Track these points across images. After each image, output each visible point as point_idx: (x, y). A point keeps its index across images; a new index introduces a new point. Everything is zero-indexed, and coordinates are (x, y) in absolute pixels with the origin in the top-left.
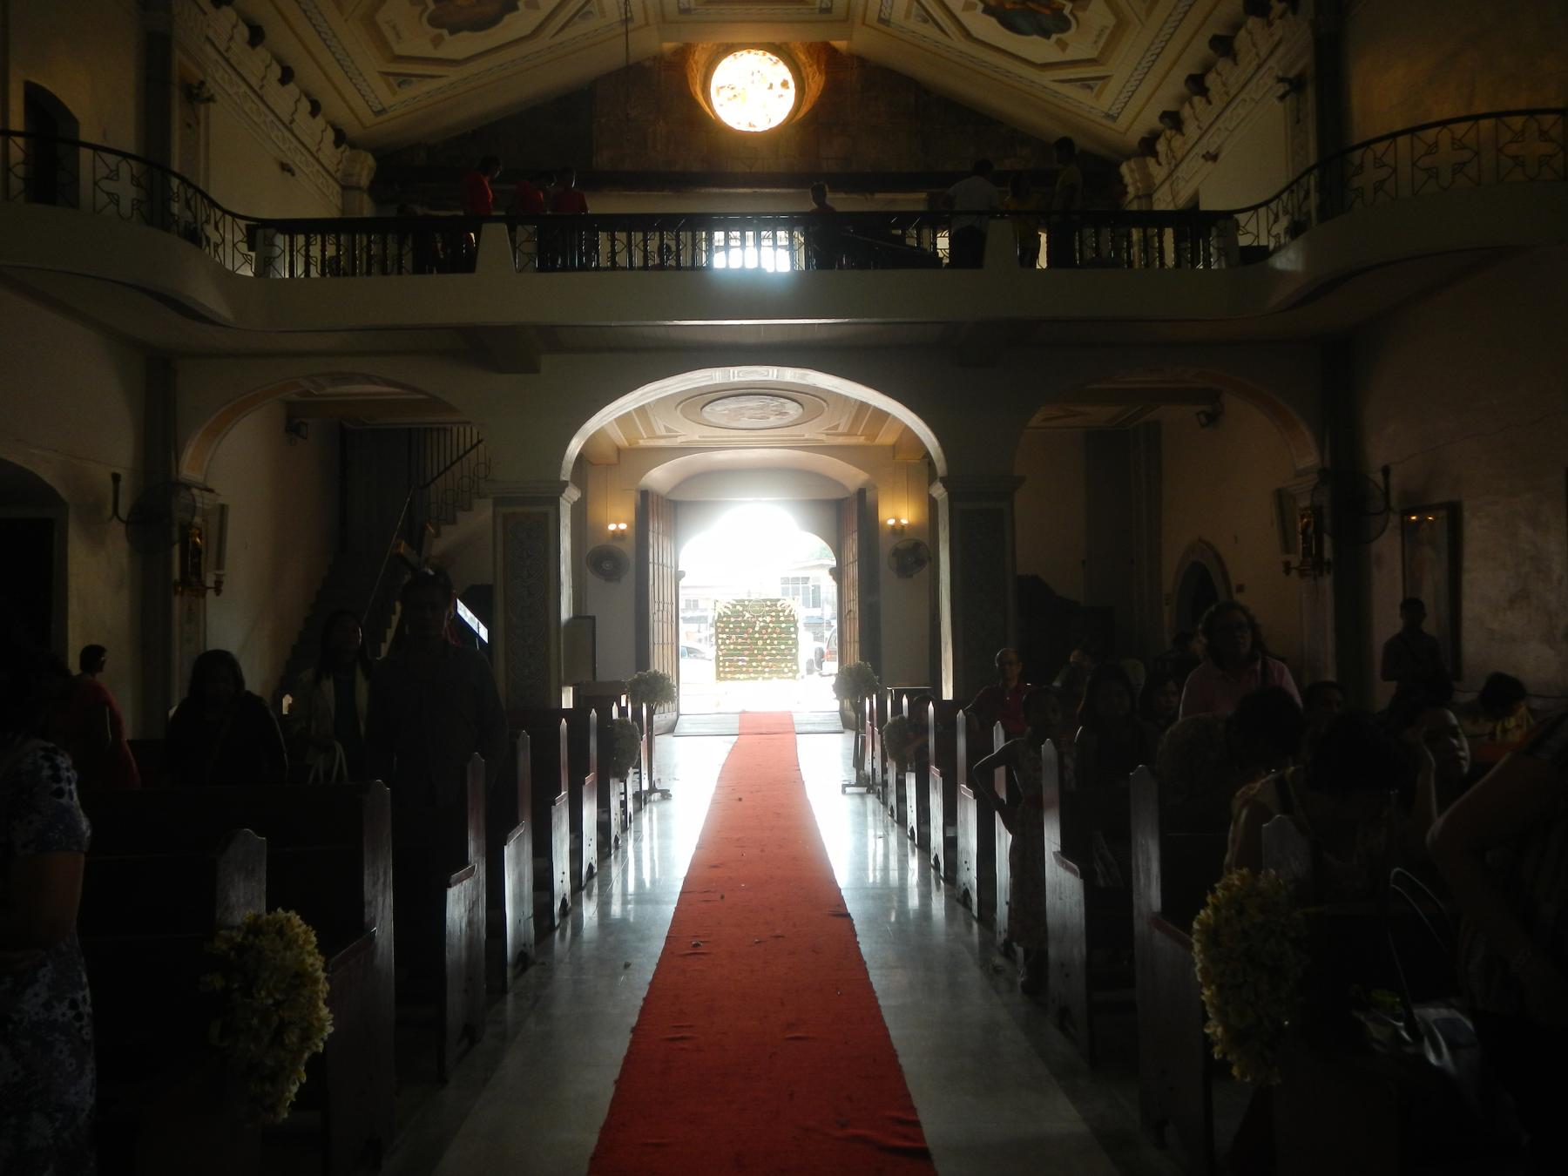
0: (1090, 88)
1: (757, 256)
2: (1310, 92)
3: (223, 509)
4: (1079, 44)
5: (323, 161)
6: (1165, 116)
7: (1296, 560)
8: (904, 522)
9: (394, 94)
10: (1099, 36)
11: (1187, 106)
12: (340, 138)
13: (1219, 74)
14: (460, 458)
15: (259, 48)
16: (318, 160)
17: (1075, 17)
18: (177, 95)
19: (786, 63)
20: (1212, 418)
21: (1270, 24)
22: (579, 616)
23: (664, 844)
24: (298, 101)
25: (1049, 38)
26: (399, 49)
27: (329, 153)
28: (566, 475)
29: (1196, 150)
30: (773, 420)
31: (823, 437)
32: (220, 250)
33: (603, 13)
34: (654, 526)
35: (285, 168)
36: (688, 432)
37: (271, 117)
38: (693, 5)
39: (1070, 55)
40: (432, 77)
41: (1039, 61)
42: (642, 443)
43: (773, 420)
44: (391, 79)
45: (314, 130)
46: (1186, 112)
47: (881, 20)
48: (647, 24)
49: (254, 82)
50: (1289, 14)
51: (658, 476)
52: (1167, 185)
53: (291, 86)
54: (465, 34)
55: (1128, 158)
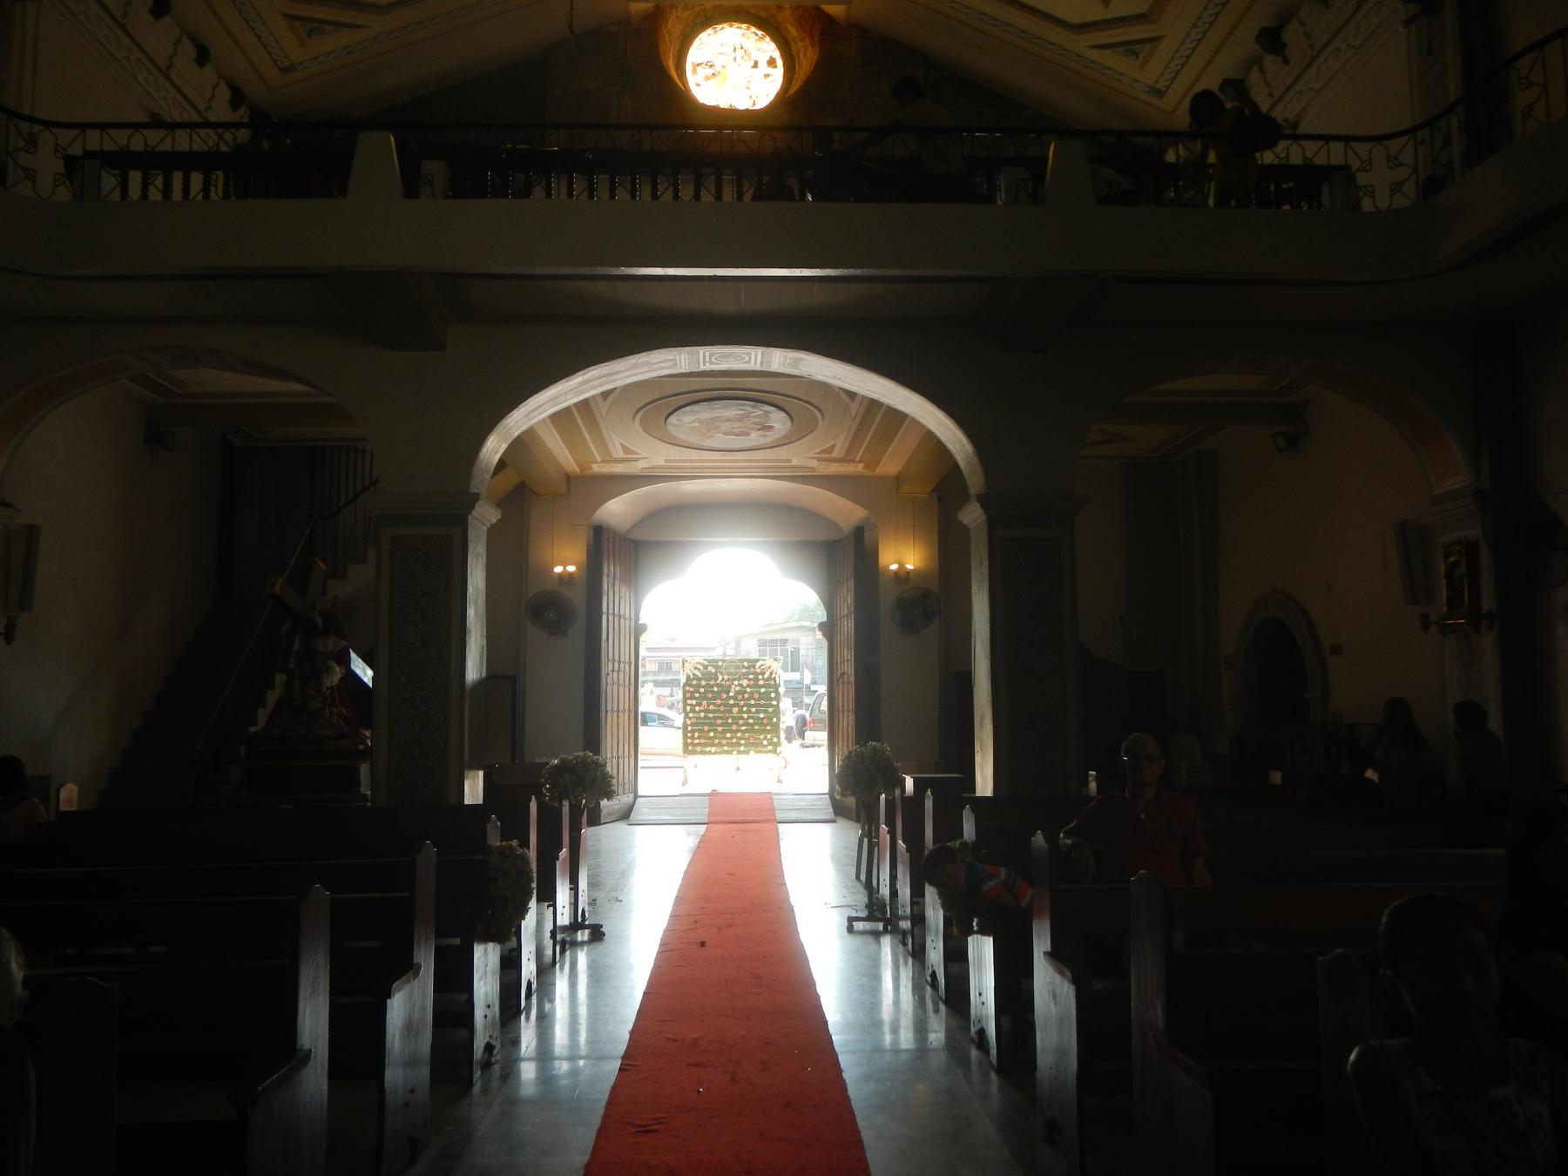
0: (1136, 54)
3: (32, 532)
8: (910, 567)
11: (1256, 69)
13: (1301, 23)
19: (773, 39)
22: (492, 678)
30: (755, 438)
31: (814, 463)
34: (609, 570)
36: (652, 454)
40: (352, 26)
42: (597, 468)
43: (755, 438)
44: (297, 23)
51: (617, 510)
53: (167, 20)
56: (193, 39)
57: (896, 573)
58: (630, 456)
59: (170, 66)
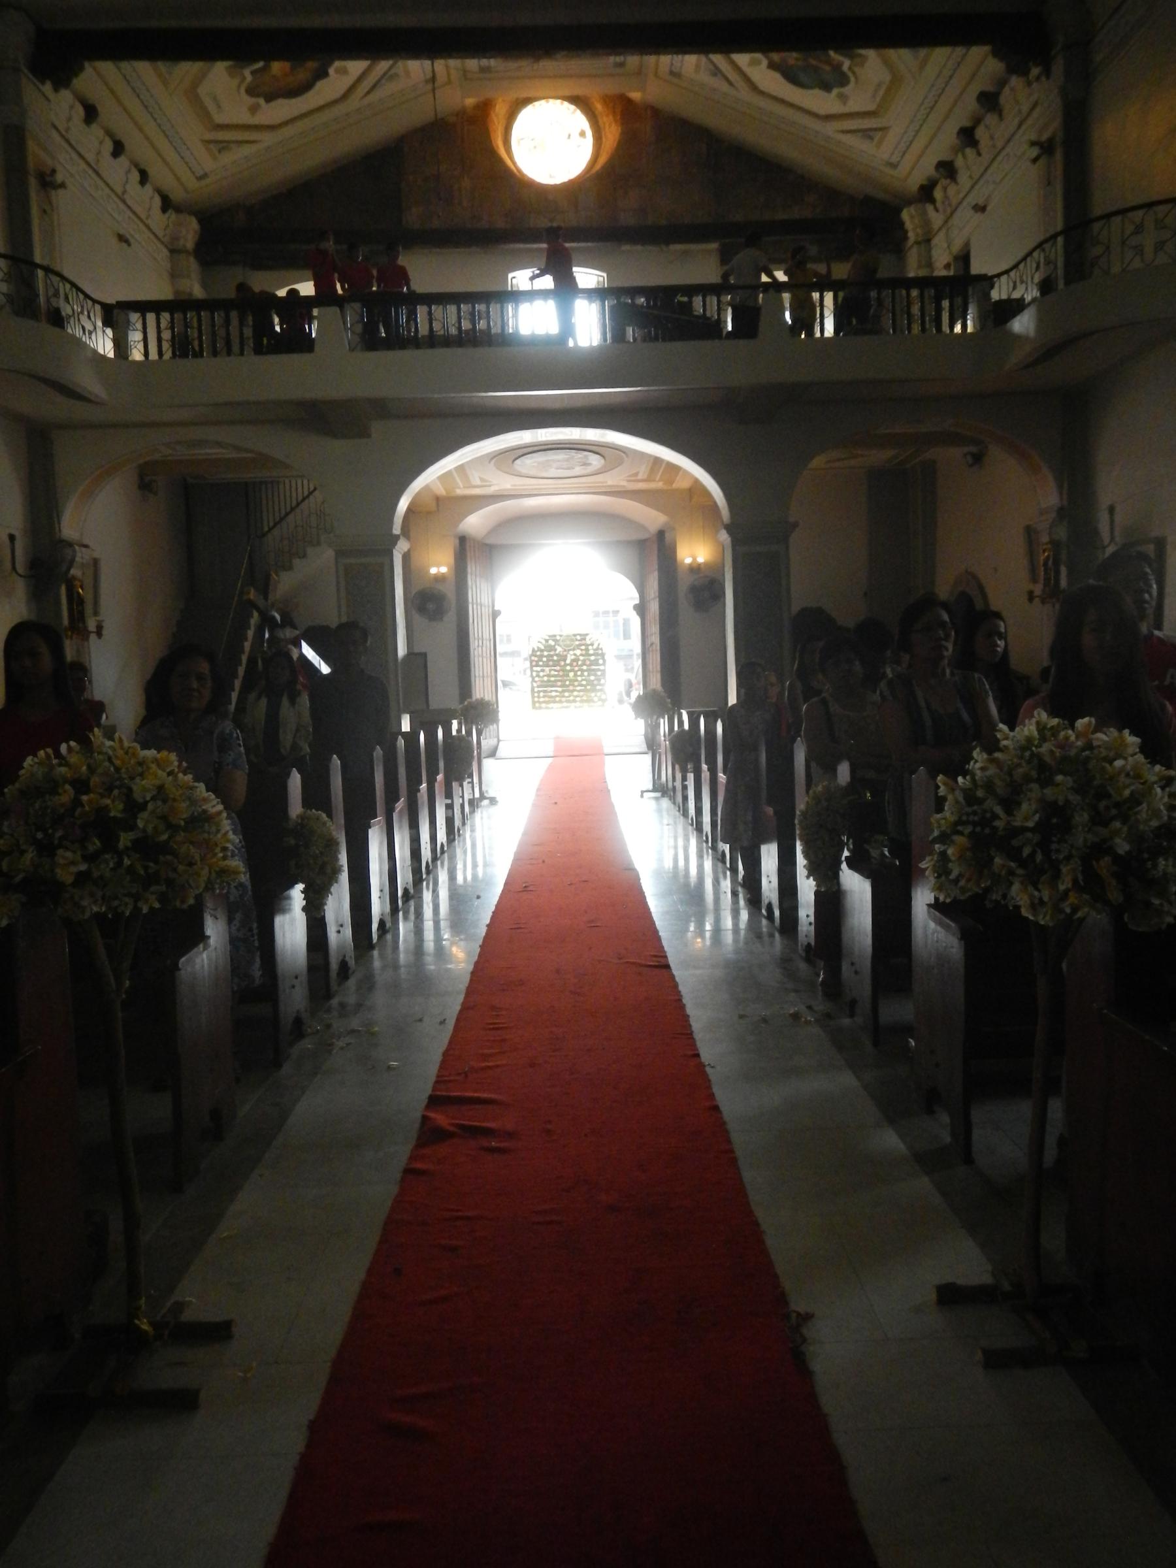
0: (871, 138)
1: (557, 313)
2: (1059, 156)
3: (96, 562)
4: (858, 98)
7: (1038, 589)
8: (701, 560)
10: (876, 91)
11: (960, 156)
12: (167, 204)
14: (292, 509)
15: (94, 126)
17: (854, 73)
18: (33, 182)
20: (978, 459)
23: (493, 838)
26: (219, 119)
27: (158, 219)
29: (965, 203)
30: (578, 470)
32: (93, 337)
35: (122, 239)
36: (501, 482)
39: (853, 106)
40: (247, 142)
42: (459, 492)
44: (212, 146)
45: (145, 199)
46: (959, 162)
47: (672, 73)
48: (449, 82)
49: (90, 157)
50: (1043, 79)
51: (475, 523)
52: (942, 234)
54: (280, 101)
55: (909, 203)
56: (136, 165)
57: (690, 565)
58: (485, 483)
59: (125, 192)
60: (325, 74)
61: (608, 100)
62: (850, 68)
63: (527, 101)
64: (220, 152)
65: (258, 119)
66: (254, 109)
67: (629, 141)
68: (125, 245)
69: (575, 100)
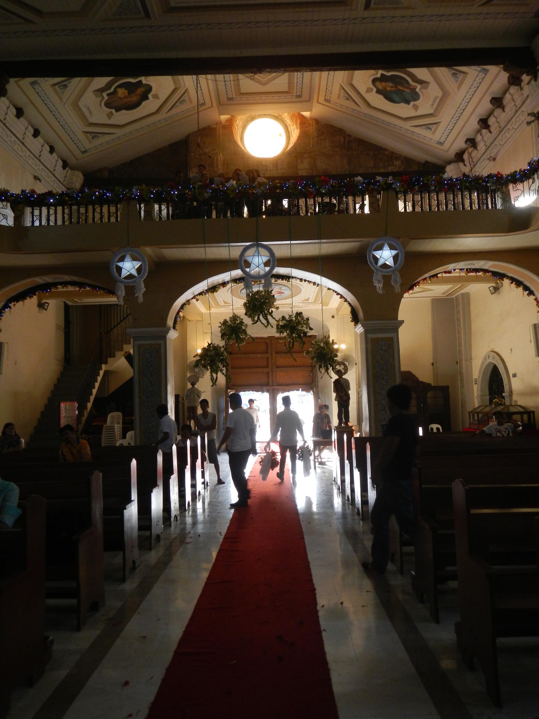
0: (431, 129)
4: (424, 105)
5: (56, 175)
6: (468, 140)
9: (90, 142)
10: (434, 101)
11: (479, 134)
12: (65, 165)
15: (22, 119)
16: (54, 175)
20: (496, 289)
21: (521, 89)
24: (43, 146)
25: (409, 104)
26: (92, 120)
28: (170, 322)
29: (484, 156)
33: (191, 101)
37: (28, 153)
38: (234, 96)
39: (420, 112)
41: (404, 117)
44: (88, 134)
46: (479, 138)
50: (533, 82)
53: (39, 138)
54: (124, 111)
55: (449, 162)
56: (47, 144)
60: (147, 98)
61: (292, 117)
62: (420, 90)
63: (253, 119)
64: (93, 138)
65: (112, 121)
66: (110, 115)
67: (303, 135)
68: (38, 181)
69: (277, 118)
